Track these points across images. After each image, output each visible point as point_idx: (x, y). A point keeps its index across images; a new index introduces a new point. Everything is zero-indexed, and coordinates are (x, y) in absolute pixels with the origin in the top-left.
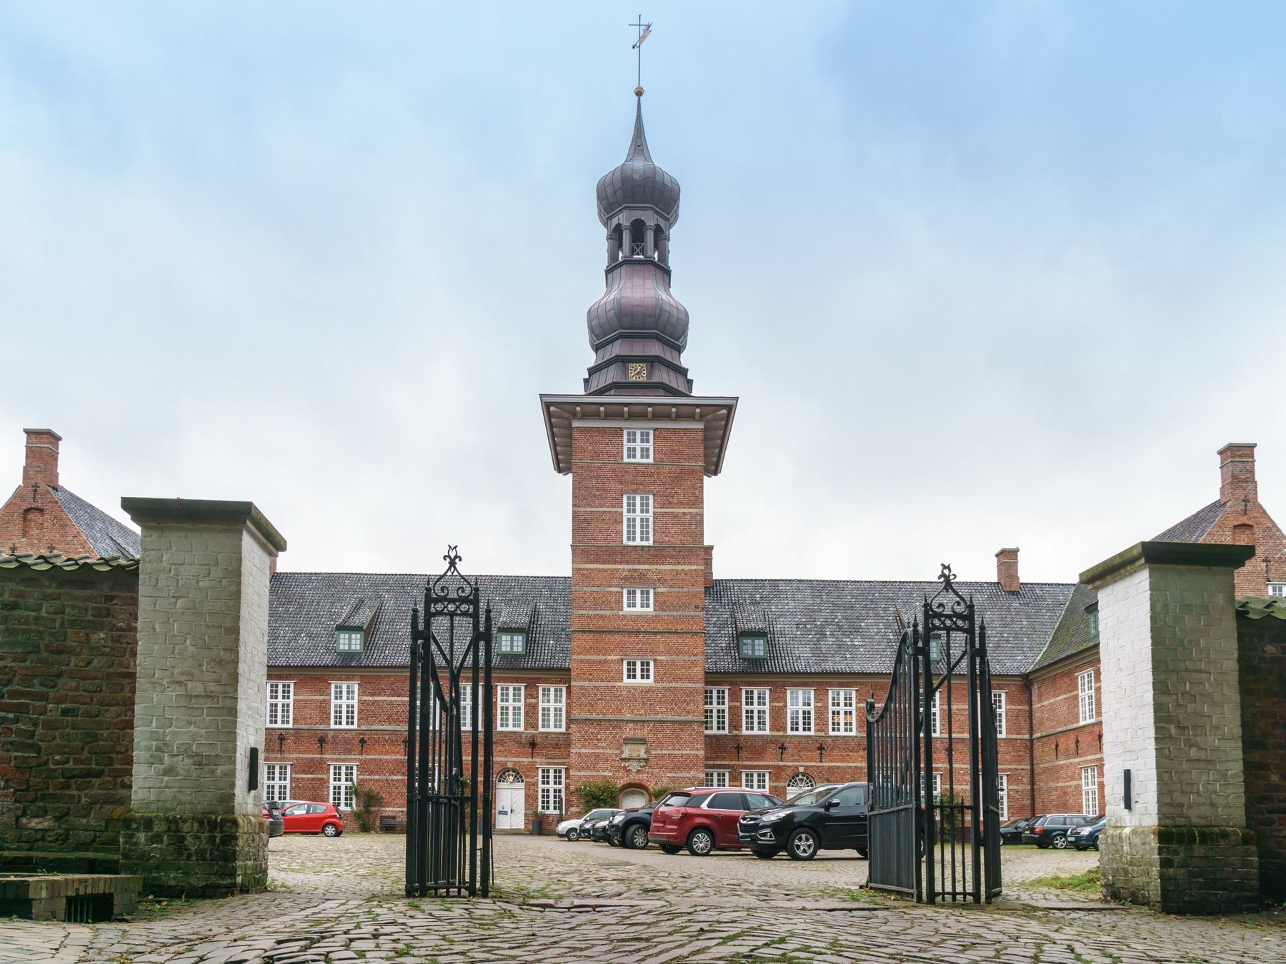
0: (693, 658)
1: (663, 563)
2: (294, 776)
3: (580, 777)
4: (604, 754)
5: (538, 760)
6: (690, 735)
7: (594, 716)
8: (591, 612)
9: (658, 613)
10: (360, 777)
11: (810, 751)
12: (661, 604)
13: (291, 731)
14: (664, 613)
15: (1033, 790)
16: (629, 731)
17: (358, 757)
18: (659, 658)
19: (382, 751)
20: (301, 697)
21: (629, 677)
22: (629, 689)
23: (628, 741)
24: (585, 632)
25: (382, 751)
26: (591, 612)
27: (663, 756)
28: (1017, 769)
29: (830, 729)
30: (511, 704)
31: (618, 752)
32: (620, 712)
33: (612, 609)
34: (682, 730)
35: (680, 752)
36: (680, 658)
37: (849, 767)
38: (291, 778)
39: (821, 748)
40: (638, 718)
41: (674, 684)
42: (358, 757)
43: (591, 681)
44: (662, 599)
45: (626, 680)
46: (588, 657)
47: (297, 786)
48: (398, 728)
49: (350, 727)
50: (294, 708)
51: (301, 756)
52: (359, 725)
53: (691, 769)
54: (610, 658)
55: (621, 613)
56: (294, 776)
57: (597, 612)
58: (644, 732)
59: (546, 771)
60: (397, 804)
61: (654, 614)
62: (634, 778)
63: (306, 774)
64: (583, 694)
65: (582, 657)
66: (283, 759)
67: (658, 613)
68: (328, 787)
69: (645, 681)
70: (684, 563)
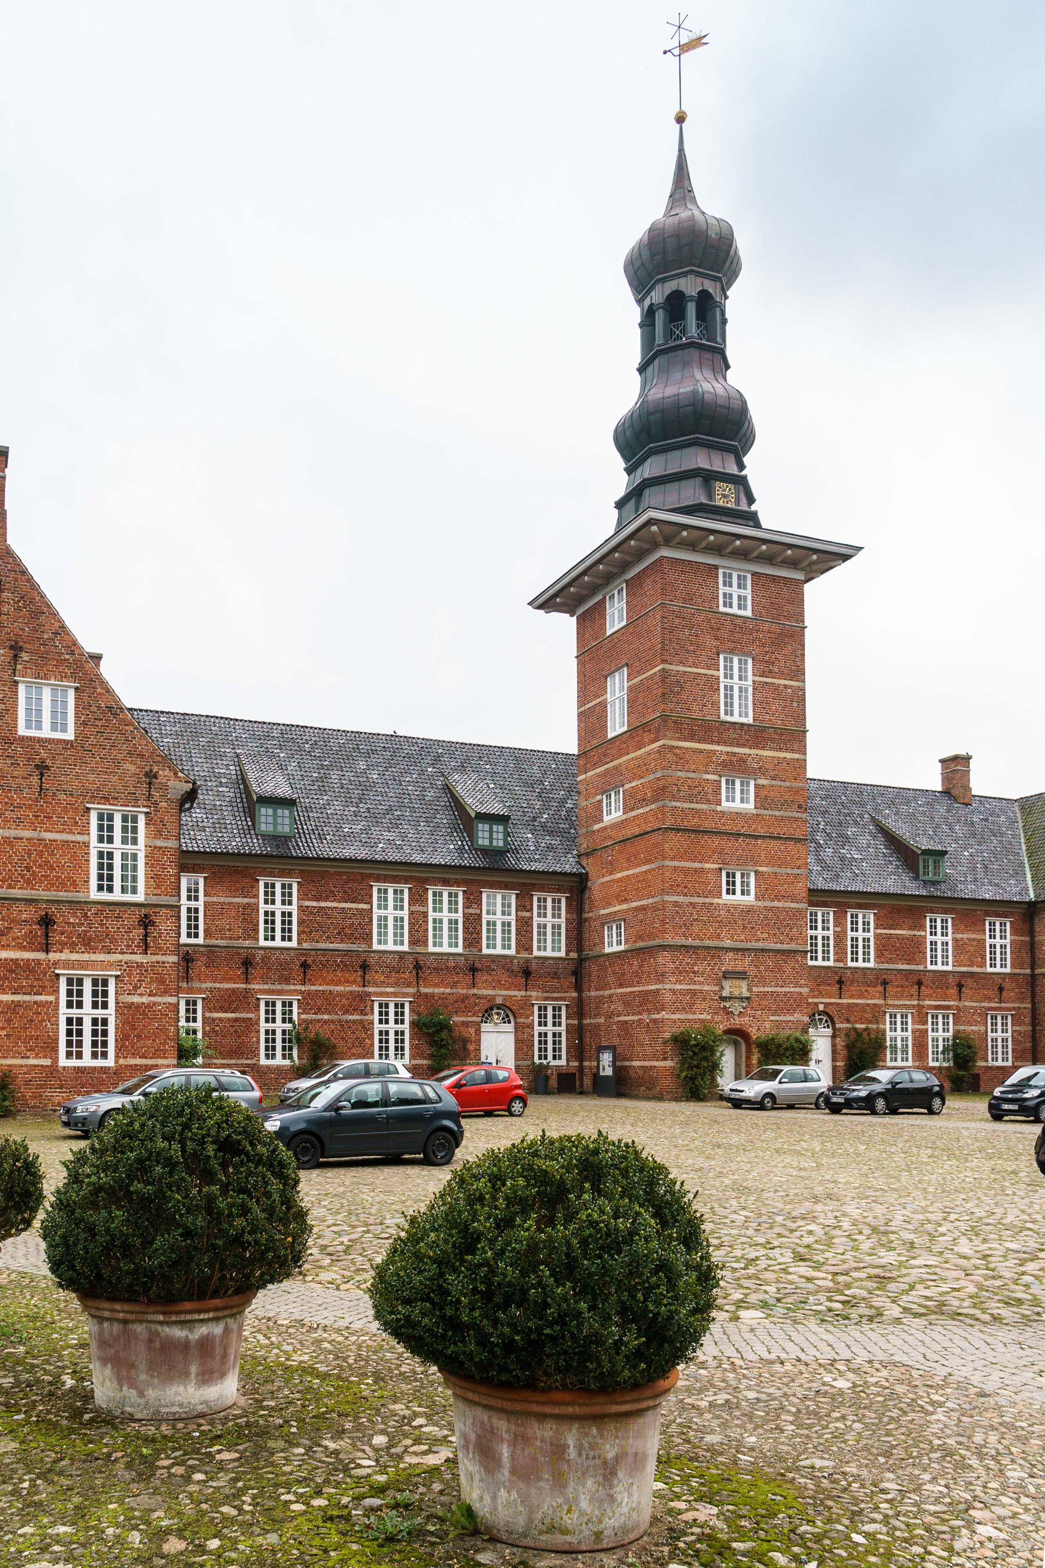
0: (796, 871)
1: (763, 748)
2: (208, 1015)
3: (675, 1021)
4: (701, 991)
5: (533, 994)
6: (793, 968)
7: (690, 942)
8: (686, 805)
9: (759, 811)
10: (303, 1016)
11: (829, 985)
12: (762, 801)
13: (202, 949)
14: (765, 812)
15: (1034, 1031)
16: (729, 962)
17: (298, 987)
18: (761, 869)
19: (332, 980)
20: (215, 899)
21: (728, 893)
22: (730, 908)
23: (727, 975)
24: (678, 830)
25: (332, 980)
26: (686, 805)
27: (765, 994)
28: (1019, 1008)
29: (849, 959)
30: (391, 912)
31: (716, 988)
32: (718, 937)
33: (709, 802)
34: (785, 962)
35: (783, 990)
36: (783, 870)
37: (868, 1005)
38: (204, 1018)
39: (840, 982)
40: (739, 945)
41: (776, 904)
42: (298, 987)
43: (685, 895)
44: (764, 793)
45: (724, 896)
46: (683, 864)
47: (213, 1030)
48: (354, 947)
49: (287, 944)
50: (205, 915)
51: (218, 985)
52: (299, 942)
53: (795, 1011)
54: (707, 866)
55: (719, 808)
56: (208, 1015)
57: (693, 806)
58: (744, 963)
59: (543, 1009)
60: (354, 1055)
61: (755, 812)
62: (737, 1022)
63: (226, 1012)
64: (677, 912)
65: (676, 863)
66: (190, 991)
67: (759, 811)
68: (258, 1031)
69: (745, 898)
70: (787, 750)
